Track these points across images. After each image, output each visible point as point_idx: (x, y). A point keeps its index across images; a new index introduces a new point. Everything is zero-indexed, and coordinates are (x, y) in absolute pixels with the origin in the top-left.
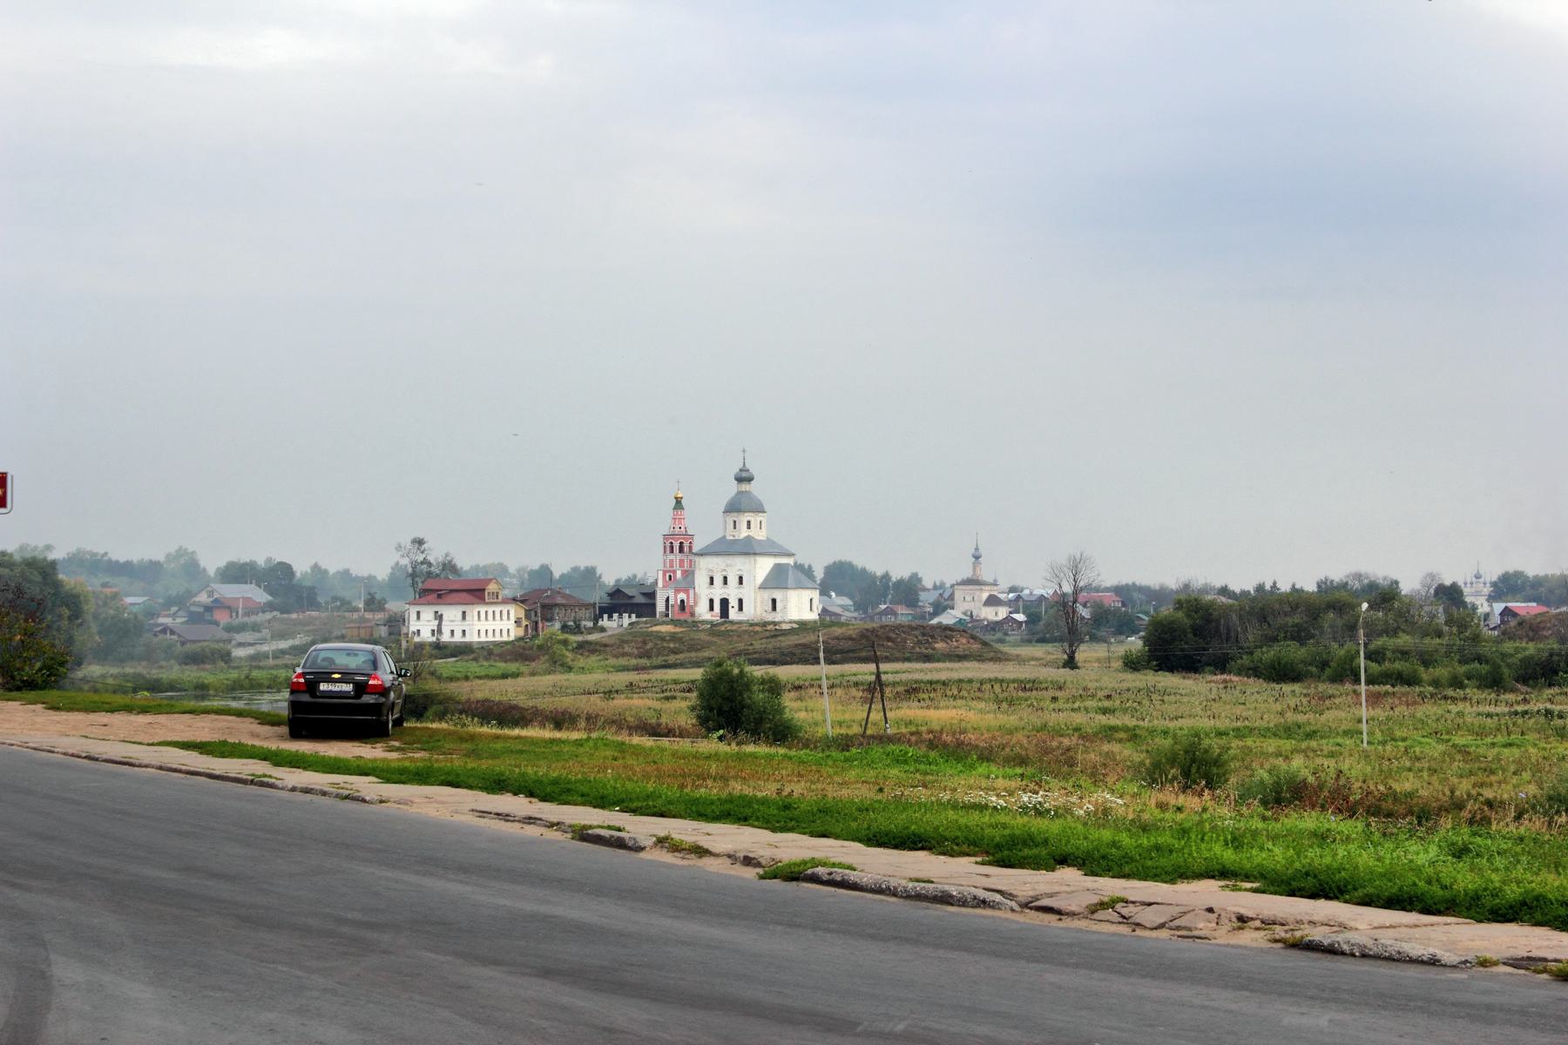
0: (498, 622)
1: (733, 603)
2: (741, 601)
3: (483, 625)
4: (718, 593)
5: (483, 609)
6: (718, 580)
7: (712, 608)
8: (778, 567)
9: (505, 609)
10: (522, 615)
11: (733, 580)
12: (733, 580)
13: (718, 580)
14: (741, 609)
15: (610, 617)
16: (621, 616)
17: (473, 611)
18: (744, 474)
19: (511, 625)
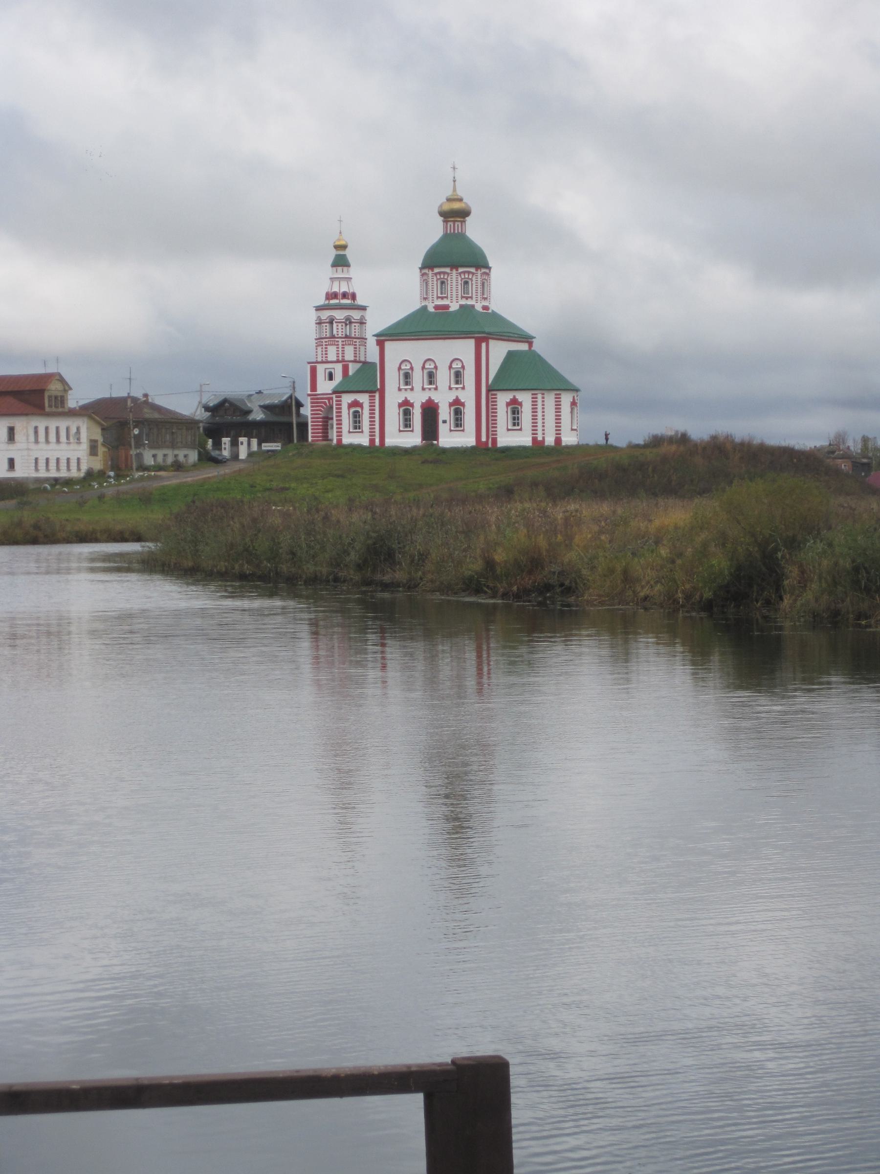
0: (63, 446)
1: (445, 413)
3: (44, 451)
4: (418, 398)
5: (41, 423)
7: (407, 423)
8: (511, 355)
9: (74, 424)
10: (98, 436)
11: (444, 377)
12: (444, 377)
13: (418, 378)
14: (458, 422)
15: (218, 445)
16: (235, 444)
17: (24, 426)
18: (456, 206)
19: (82, 451)
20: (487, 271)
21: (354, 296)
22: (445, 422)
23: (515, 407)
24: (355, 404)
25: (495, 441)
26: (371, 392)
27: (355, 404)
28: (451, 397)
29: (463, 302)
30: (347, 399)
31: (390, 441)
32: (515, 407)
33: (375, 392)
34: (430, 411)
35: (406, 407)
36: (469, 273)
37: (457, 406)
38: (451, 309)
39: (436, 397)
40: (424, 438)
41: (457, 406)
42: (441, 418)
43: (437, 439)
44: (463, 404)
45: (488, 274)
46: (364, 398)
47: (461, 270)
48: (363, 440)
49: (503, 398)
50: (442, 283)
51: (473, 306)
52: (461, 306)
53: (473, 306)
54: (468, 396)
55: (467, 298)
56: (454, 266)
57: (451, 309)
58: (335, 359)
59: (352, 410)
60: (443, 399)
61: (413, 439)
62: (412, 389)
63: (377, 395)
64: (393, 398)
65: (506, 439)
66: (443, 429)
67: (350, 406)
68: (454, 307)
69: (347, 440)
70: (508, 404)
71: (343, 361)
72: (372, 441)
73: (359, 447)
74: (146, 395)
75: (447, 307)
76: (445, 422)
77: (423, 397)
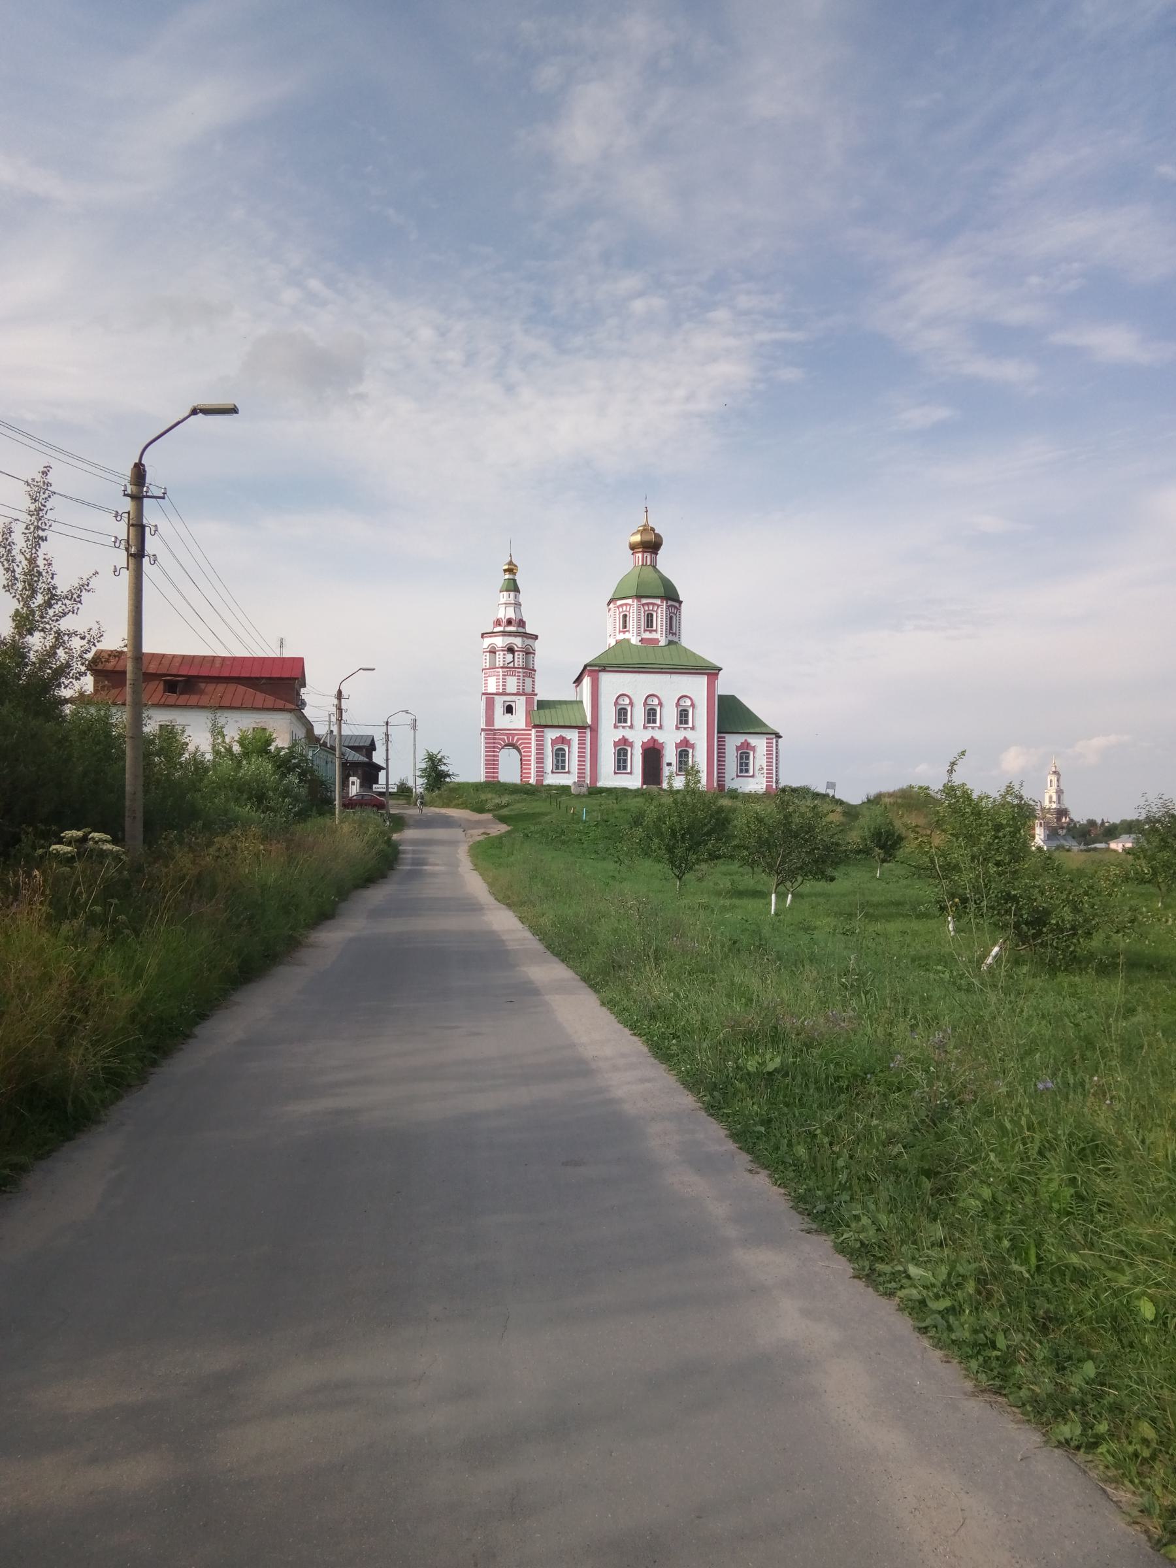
1: (670, 755)
4: (639, 736)
6: (638, 715)
7: (621, 763)
11: (669, 715)
12: (669, 715)
13: (638, 715)
21: (521, 623)
22: (669, 764)
24: (562, 740)
26: (581, 728)
28: (679, 736)
30: (551, 735)
31: (603, 783)
34: (652, 754)
39: (660, 736)
40: (644, 783)
42: (666, 760)
44: (693, 746)
45: (678, 609)
46: (573, 735)
54: (699, 737)
58: (494, 691)
60: (669, 737)
61: (633, 781)
62: (631, 727)
64: (609, 735)
65: (733, 782)
67: (554, 742)
73: (565, 789)
77: (646, 736)
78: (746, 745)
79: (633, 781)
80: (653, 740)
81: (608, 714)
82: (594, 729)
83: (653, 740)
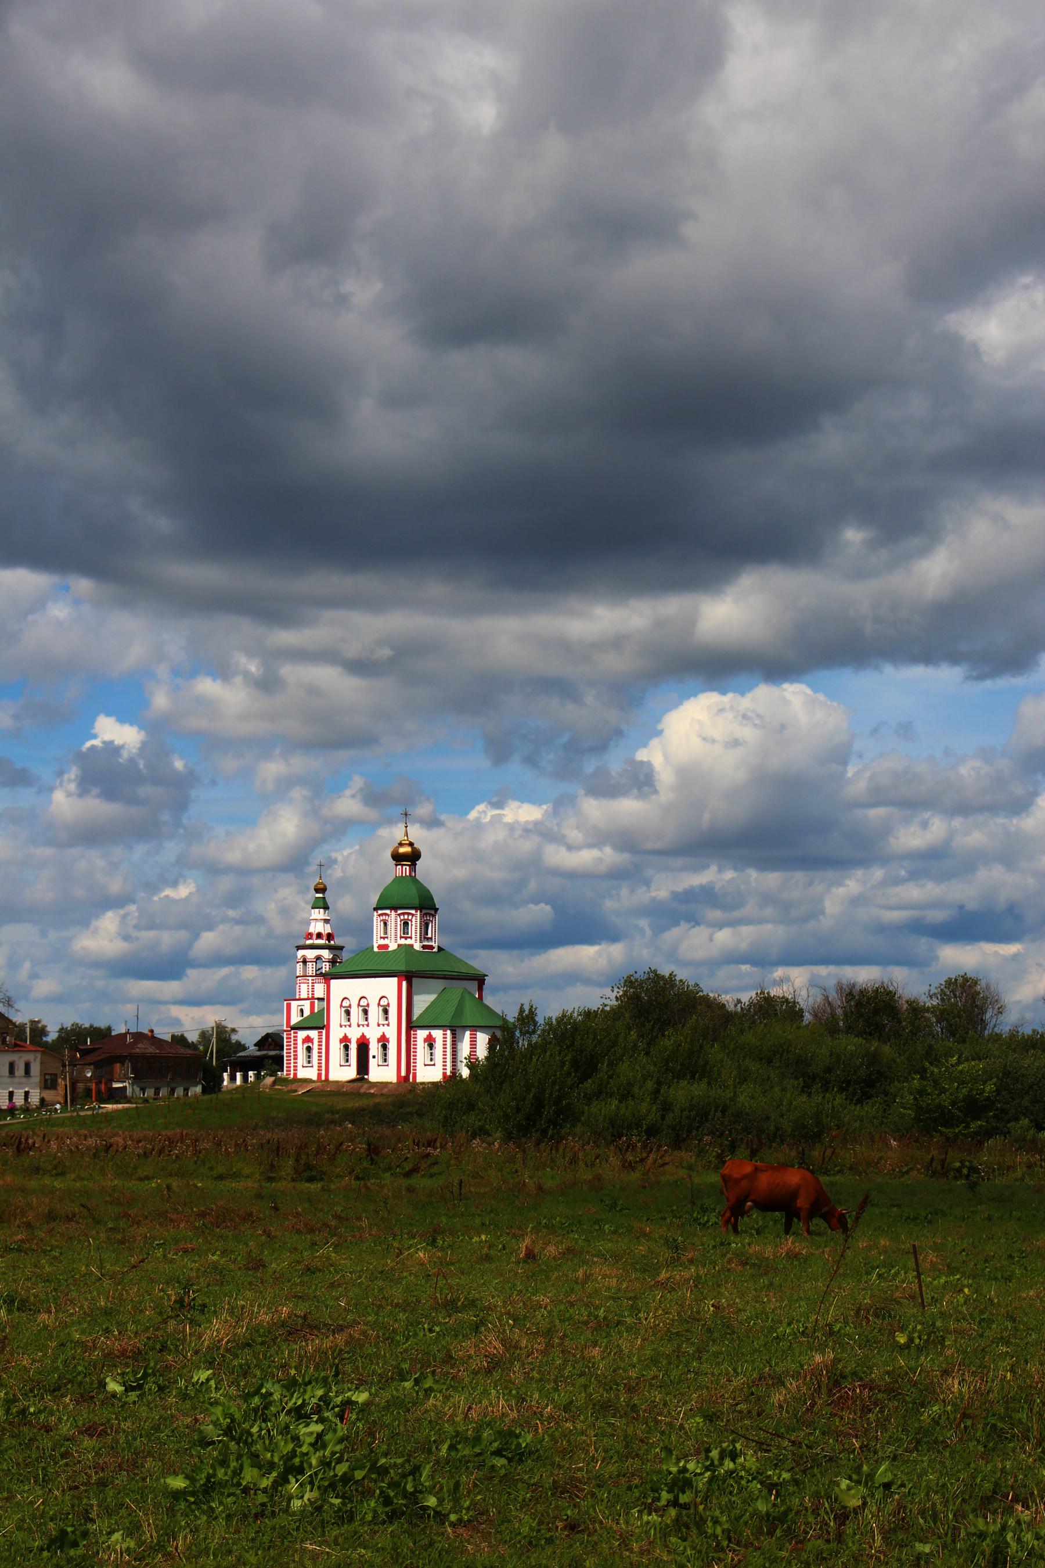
1: (374, 1049)
2: (385, 1047)
4: (354, 1034)
11: (374, 1012)
12: (374, 1012)
13: (356, 1013)
20: (433, 912)
22: (374, 1057)
23: (430, 1042)
24: (308, 1039)
25: (415, 1075)
27: (308, 1039)
29: (403, 942)
30: (302, 1034)
31: (331, 1078)
32: (430, 1042)
33: (322, 1028)
34: (363, 1046)
35: (345, 1040)
36: (408, 914)
37: (384, 1041)
38: (390, 949)
40: (358, 1073)
41: (384, 1041)
42: (371, 1053)
43: (367, 1074)
46: (314, 1034)
47: (399, 912)
48: (311, 1074)
49: (421, 1034)
50: (385, 924)
51: (412, 946)
52: (399, 945)
53: (412, 946)
54: (391, 1033)
55: (406, 938)
56: (395, 908)
57: (390, 949)
59: (306, 1045)
60: (373, 1035)
63: (324, 1031)
64: (336, 1033)
66: (373, 1063)
68: (393, 947)
69: (303, 1073)
70: (425, 1040)
71: (313, 998)
72: (319, 1075)
74: (152, 1031)
75: (386, 946)
76: (374, 1057)
78: (430, 1036)
79: (350, 1073)
80: (363, 1036)
81: (336, 1015)
82: (327, 1027)
83: (363, 1036)
